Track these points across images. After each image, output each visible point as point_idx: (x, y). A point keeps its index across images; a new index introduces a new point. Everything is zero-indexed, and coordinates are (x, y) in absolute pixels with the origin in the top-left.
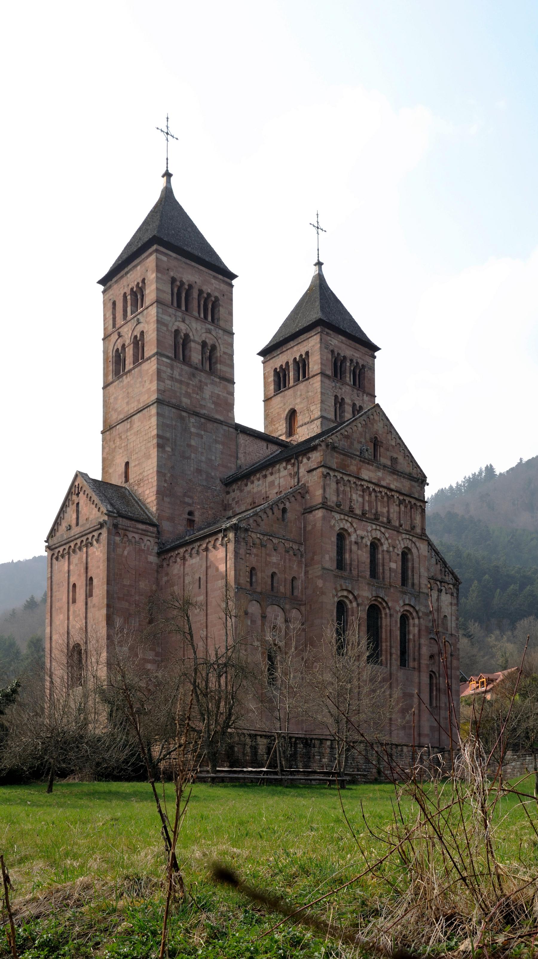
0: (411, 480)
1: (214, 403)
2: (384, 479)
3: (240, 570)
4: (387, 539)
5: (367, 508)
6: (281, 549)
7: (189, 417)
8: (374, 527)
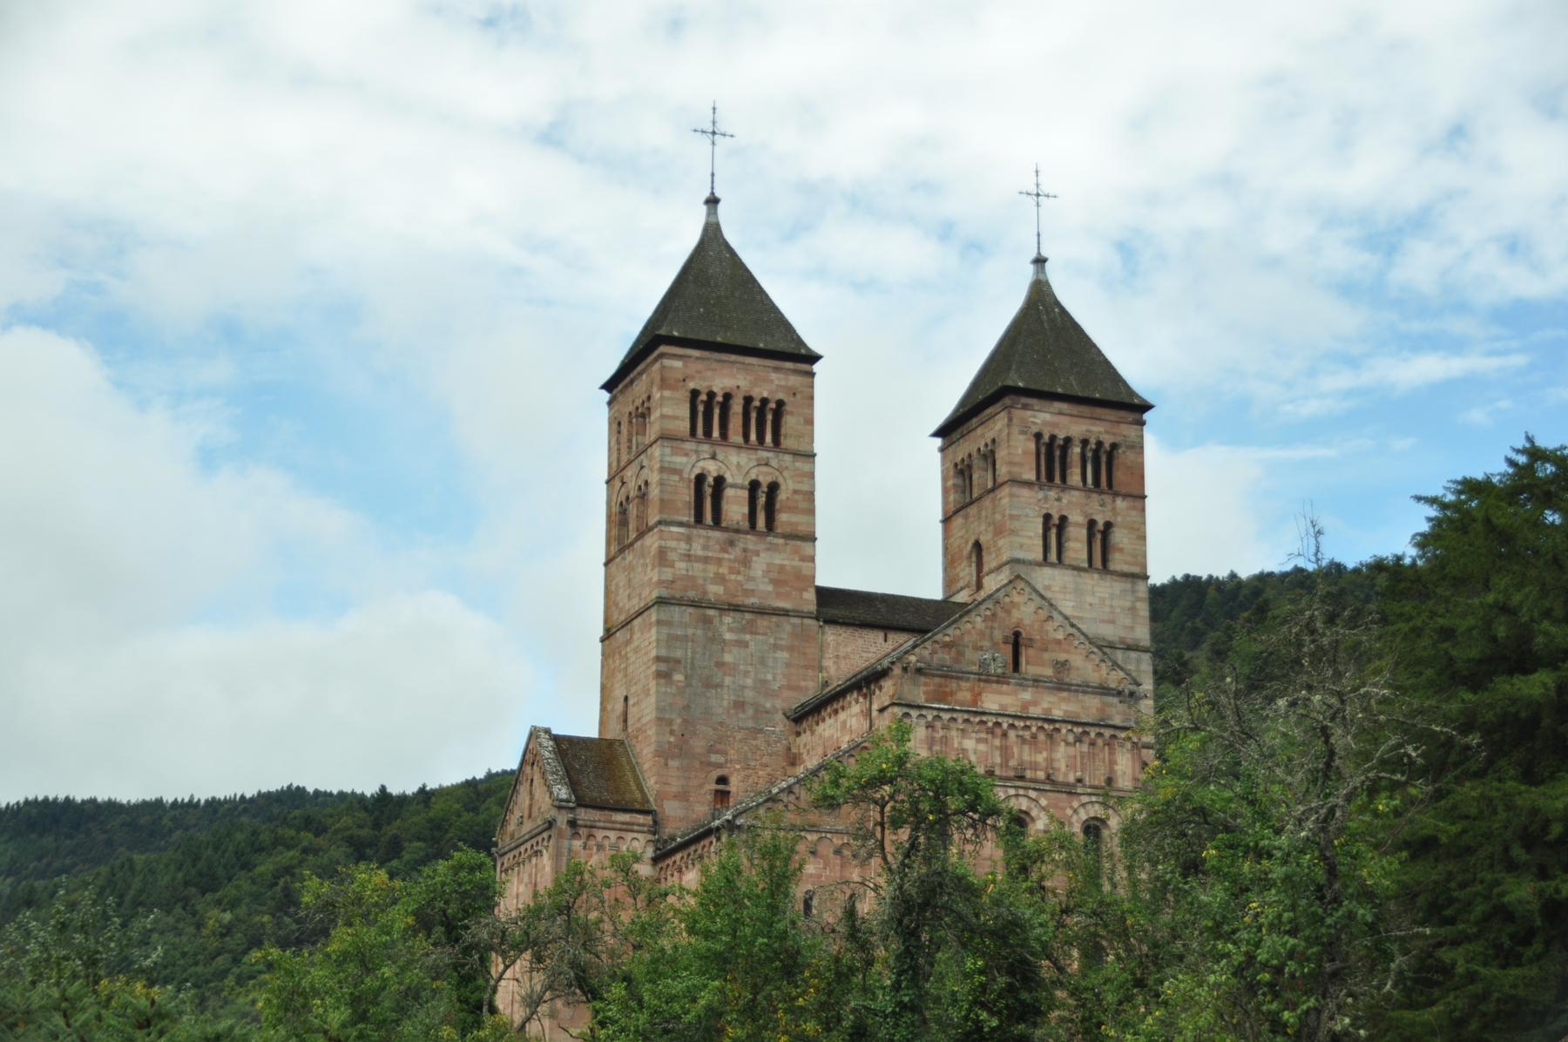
1: (776, 582)
2: (1035, 703)
6: (826, 850)
8: (1012, 792)
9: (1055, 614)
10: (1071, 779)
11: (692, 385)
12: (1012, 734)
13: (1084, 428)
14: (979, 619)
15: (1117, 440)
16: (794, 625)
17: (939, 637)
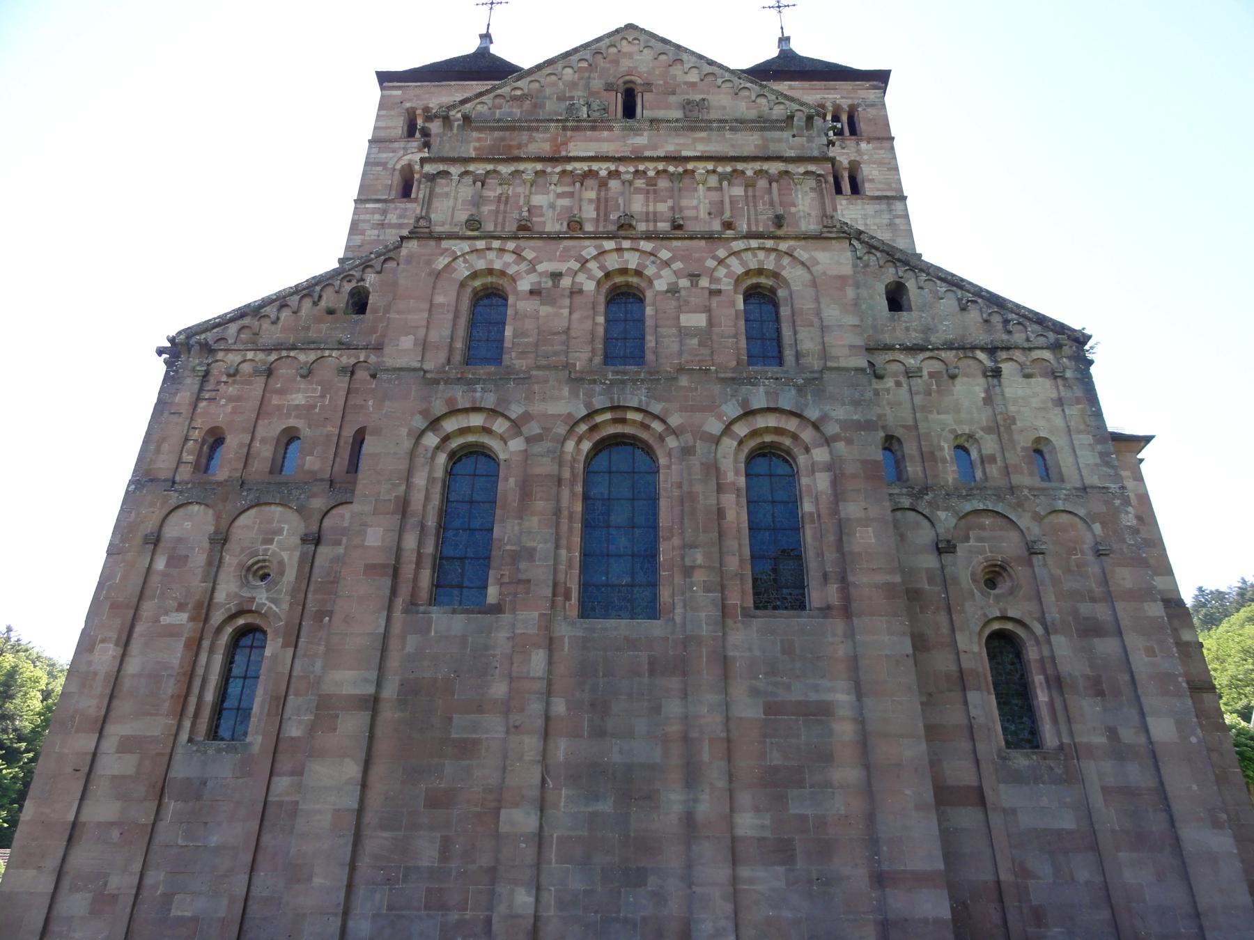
0: (762, 129)
2: (655, 148)
3: (164, 439)
4: (667, 264)
5: (589, 212)
8: (609, 245)
9: (685, 57)
10: (716, 226)
11: (408, 105)
12: (614, 184)
13: (819, 97)
14: (569, 71)
15: (856, 102)
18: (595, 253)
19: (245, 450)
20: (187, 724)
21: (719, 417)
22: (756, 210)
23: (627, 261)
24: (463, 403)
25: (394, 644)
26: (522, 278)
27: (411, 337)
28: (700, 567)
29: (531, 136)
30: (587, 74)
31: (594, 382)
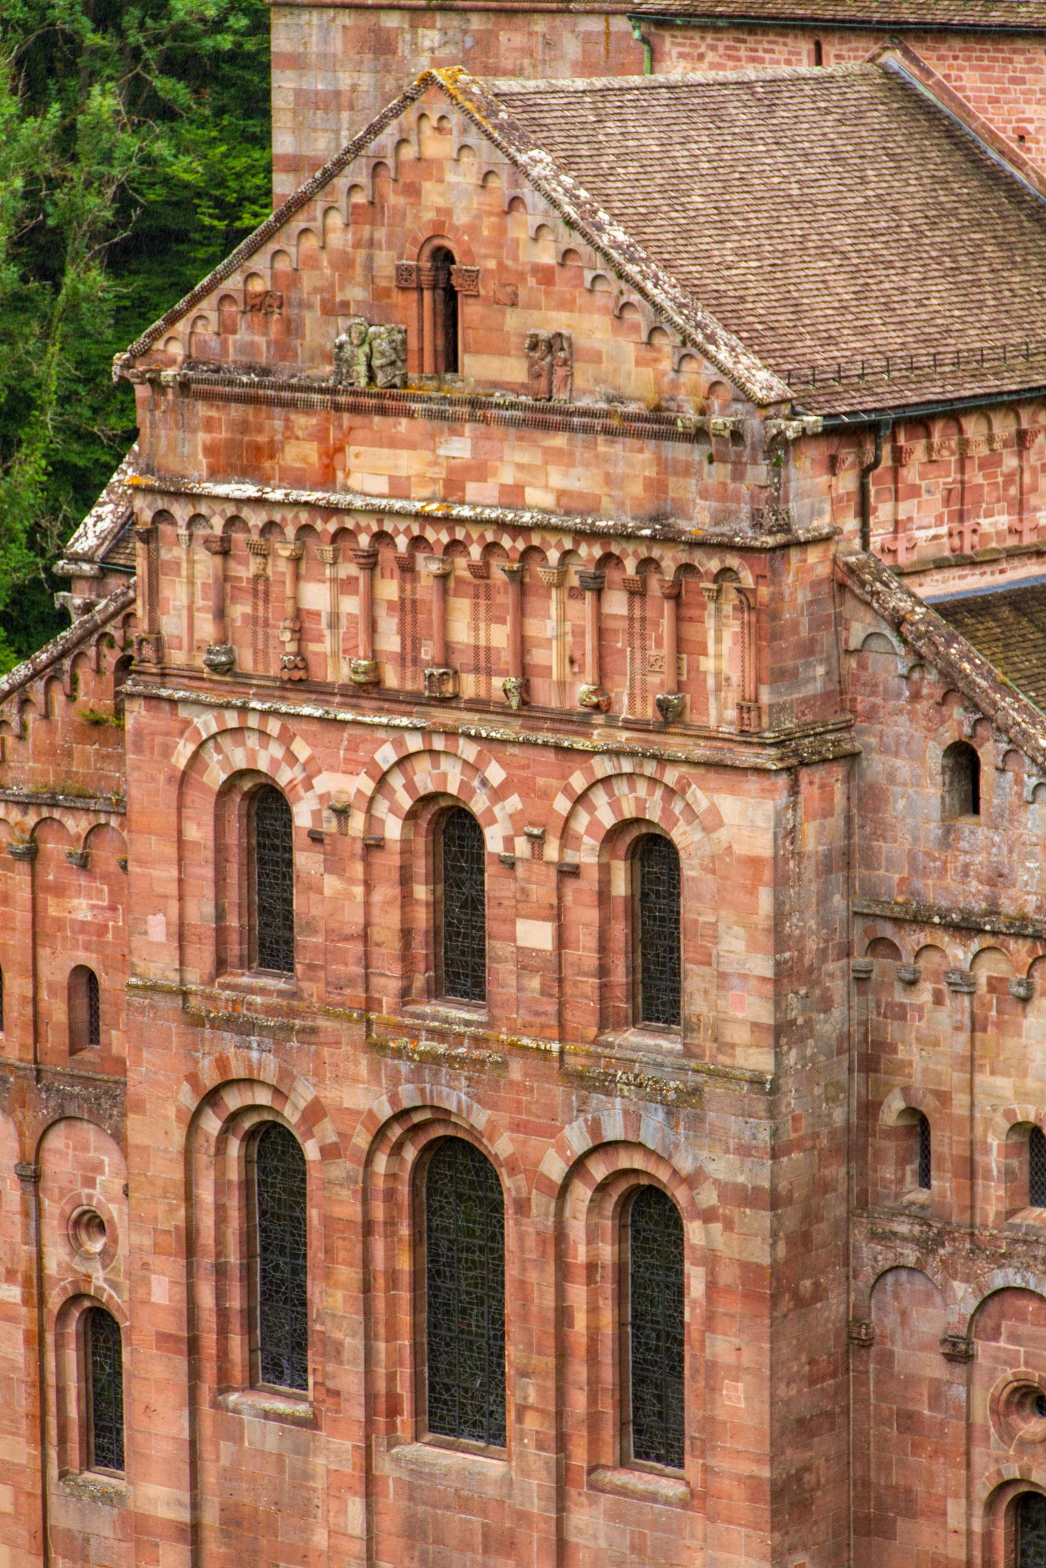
5: (390, 641)
7: (414, 27)
8: (414, 743)
16: (587, 38)
17: (233, 283)
18: (393, 758)
19: (29, 1010)
20: (53, 1453)
21: (561, 1148)
22: (644, 659)
23: (445, 775)
24: (238, 1071)
25: (207, 1450)
26: (300, 799)
27: (160, 917)
28: (531, 1408)
29: (287, 420)
30: (366, 230)
31: (398, 1053)
